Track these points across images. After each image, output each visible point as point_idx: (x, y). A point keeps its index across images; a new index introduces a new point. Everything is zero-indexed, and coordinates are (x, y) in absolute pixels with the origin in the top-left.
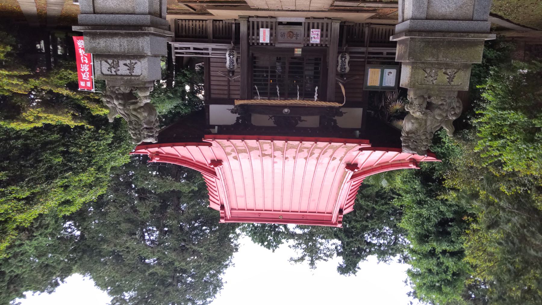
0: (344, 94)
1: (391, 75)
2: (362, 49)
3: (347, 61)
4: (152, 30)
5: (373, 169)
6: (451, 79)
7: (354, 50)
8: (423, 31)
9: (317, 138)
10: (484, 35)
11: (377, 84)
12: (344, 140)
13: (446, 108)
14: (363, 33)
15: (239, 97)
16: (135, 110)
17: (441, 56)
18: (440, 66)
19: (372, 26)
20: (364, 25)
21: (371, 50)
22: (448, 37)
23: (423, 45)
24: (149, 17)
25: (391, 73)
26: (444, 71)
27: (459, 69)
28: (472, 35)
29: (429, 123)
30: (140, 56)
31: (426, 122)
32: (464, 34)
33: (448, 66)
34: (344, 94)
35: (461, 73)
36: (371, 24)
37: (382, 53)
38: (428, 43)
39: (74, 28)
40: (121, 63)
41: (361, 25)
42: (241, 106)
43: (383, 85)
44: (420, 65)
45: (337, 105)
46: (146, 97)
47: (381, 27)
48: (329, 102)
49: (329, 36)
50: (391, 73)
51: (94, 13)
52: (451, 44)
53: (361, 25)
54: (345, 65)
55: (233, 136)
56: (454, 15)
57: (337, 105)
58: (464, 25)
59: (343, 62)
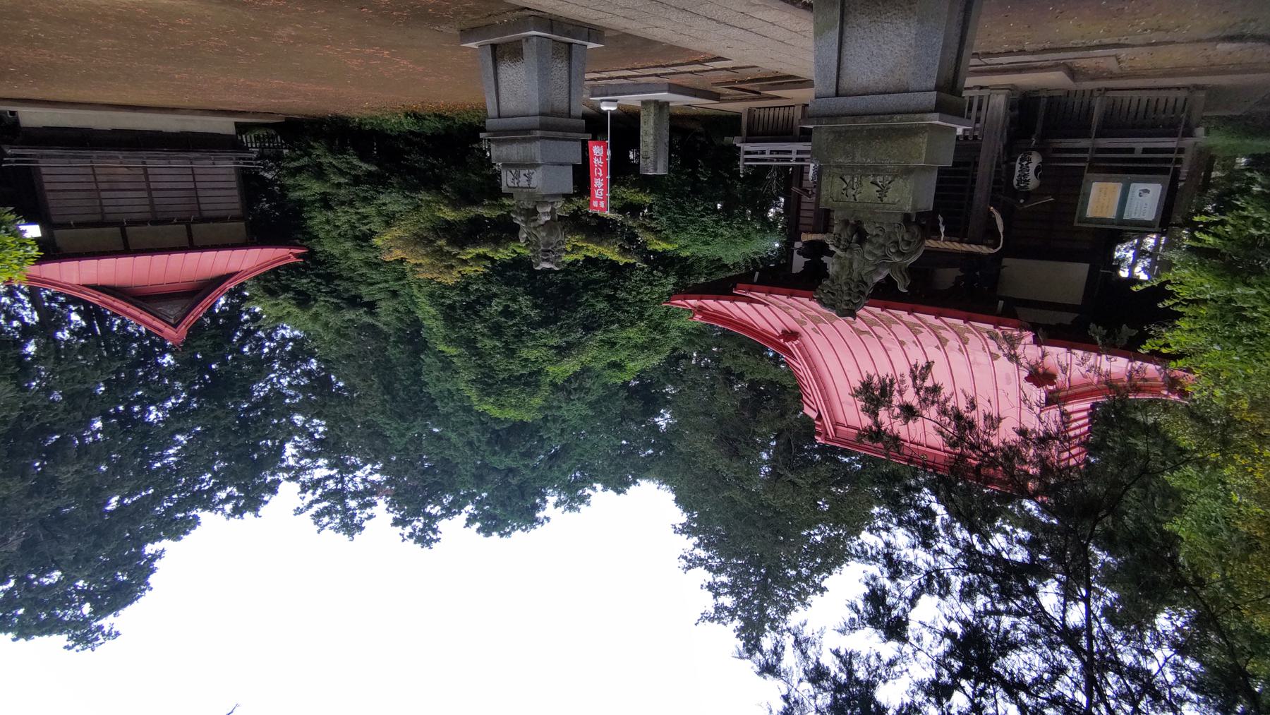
0: (1001, 231)
1: (1147, 197)
2: (1083, 143)
3: (1032, 167)
4: (538, 133)
5: (1093, 390)
6: (883, 191)
7: (1063, 146)
8: (824, 116)
9: (941, 310)
10: (918, 116)
11: (1111, 214)
12: (995, 318)
13: (881, 241)
14: (1090, 109)
15: (807, 228)
16: (535, 228)
17: (858, 155)
18: (865, 170)
19: (1110, 94)
20: (1096, 94)
21: (1104, 143)
22: (860, 123)
23: (831, 137)
24: (538, 118)
25: (1147, 191)
26: (872, 179)
27: (896, 176)
28: (899, 117)
29: (855, 265)
30: (534, 165)
31: (851, 264)
32: (887, 117)
33: (877, 170)
34: (1001, 231)
35: (899, 182)
36: (1107, 89)
37: (1132, 150)
38: (839, 134)
39: (482, 135)
40: (522, 172)
41: (1087, 95)
42: (812, 242)
43: (1126, 217)
44: (835, 170)
45: (985, 250)
46: (544, 213)
47: (1136, 95)
48: (968, 243)
49: (982, 119)
50: (1147, 191)
51: (499, 117)
52: (873, 135)
53: (1087, 95)
54: (1025, 175)
55: (777, 289)
56: (881, 86)
57: (985, 250)
58: (892, 101)
59: (1025, 169)
